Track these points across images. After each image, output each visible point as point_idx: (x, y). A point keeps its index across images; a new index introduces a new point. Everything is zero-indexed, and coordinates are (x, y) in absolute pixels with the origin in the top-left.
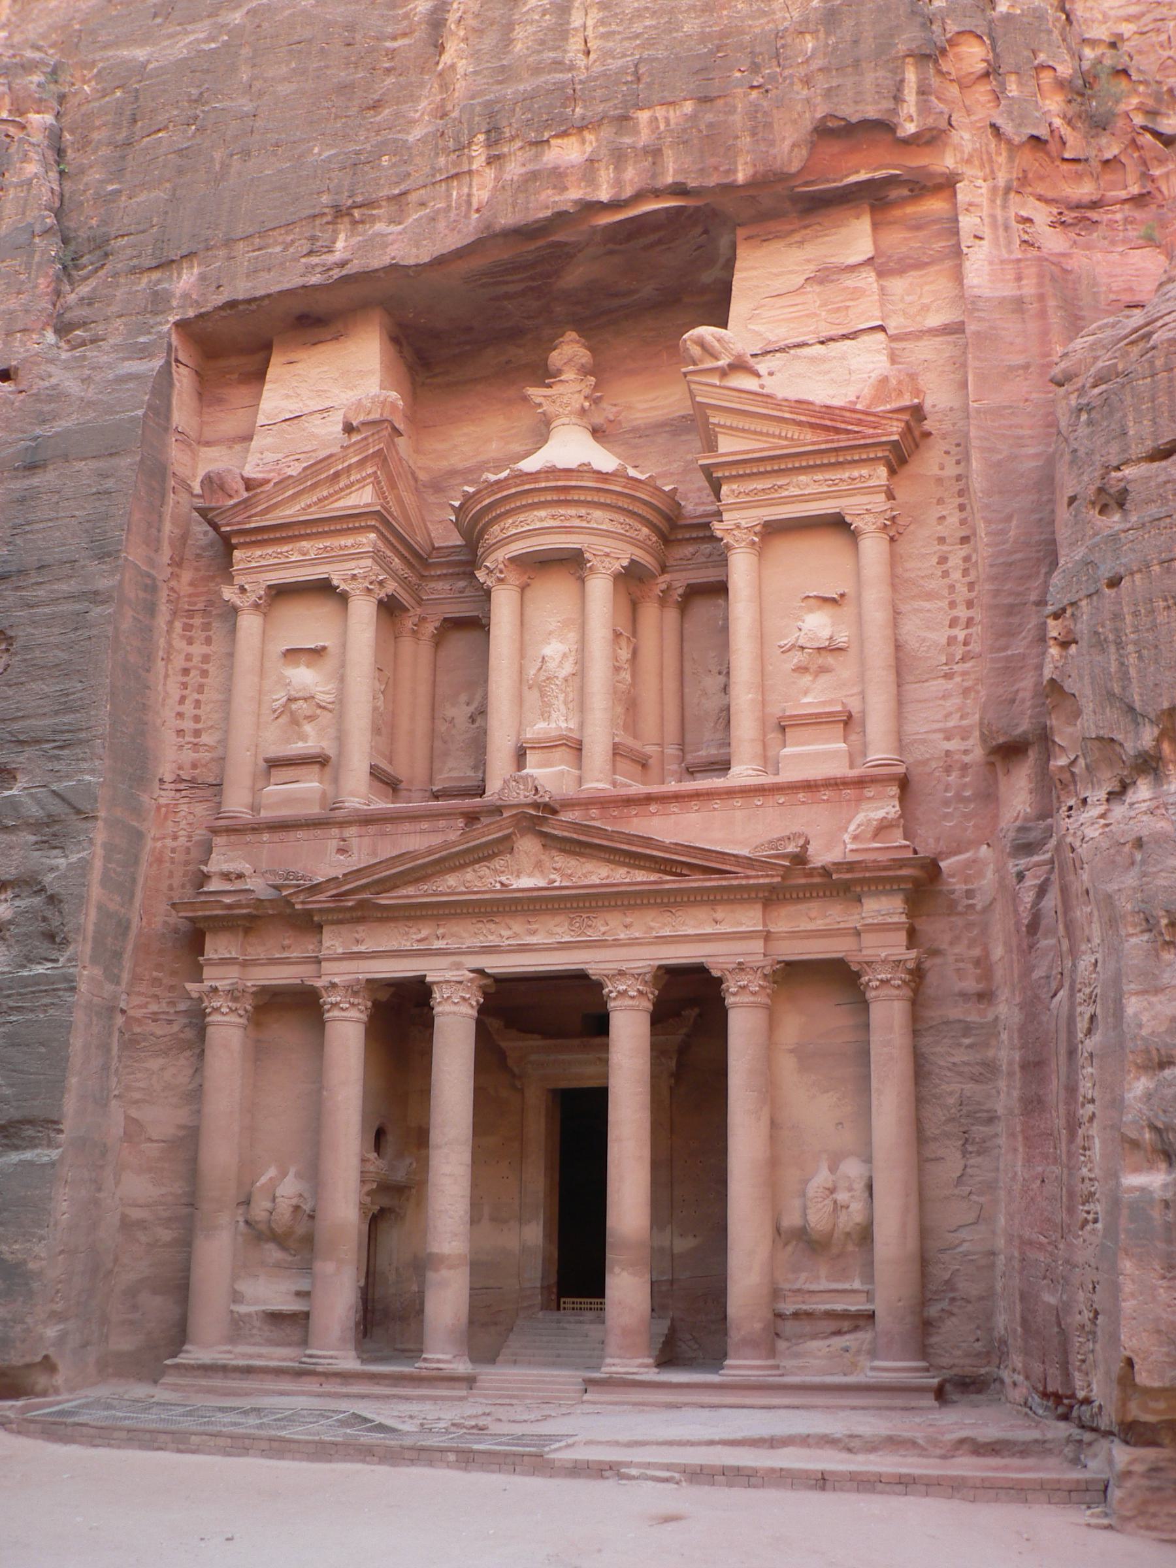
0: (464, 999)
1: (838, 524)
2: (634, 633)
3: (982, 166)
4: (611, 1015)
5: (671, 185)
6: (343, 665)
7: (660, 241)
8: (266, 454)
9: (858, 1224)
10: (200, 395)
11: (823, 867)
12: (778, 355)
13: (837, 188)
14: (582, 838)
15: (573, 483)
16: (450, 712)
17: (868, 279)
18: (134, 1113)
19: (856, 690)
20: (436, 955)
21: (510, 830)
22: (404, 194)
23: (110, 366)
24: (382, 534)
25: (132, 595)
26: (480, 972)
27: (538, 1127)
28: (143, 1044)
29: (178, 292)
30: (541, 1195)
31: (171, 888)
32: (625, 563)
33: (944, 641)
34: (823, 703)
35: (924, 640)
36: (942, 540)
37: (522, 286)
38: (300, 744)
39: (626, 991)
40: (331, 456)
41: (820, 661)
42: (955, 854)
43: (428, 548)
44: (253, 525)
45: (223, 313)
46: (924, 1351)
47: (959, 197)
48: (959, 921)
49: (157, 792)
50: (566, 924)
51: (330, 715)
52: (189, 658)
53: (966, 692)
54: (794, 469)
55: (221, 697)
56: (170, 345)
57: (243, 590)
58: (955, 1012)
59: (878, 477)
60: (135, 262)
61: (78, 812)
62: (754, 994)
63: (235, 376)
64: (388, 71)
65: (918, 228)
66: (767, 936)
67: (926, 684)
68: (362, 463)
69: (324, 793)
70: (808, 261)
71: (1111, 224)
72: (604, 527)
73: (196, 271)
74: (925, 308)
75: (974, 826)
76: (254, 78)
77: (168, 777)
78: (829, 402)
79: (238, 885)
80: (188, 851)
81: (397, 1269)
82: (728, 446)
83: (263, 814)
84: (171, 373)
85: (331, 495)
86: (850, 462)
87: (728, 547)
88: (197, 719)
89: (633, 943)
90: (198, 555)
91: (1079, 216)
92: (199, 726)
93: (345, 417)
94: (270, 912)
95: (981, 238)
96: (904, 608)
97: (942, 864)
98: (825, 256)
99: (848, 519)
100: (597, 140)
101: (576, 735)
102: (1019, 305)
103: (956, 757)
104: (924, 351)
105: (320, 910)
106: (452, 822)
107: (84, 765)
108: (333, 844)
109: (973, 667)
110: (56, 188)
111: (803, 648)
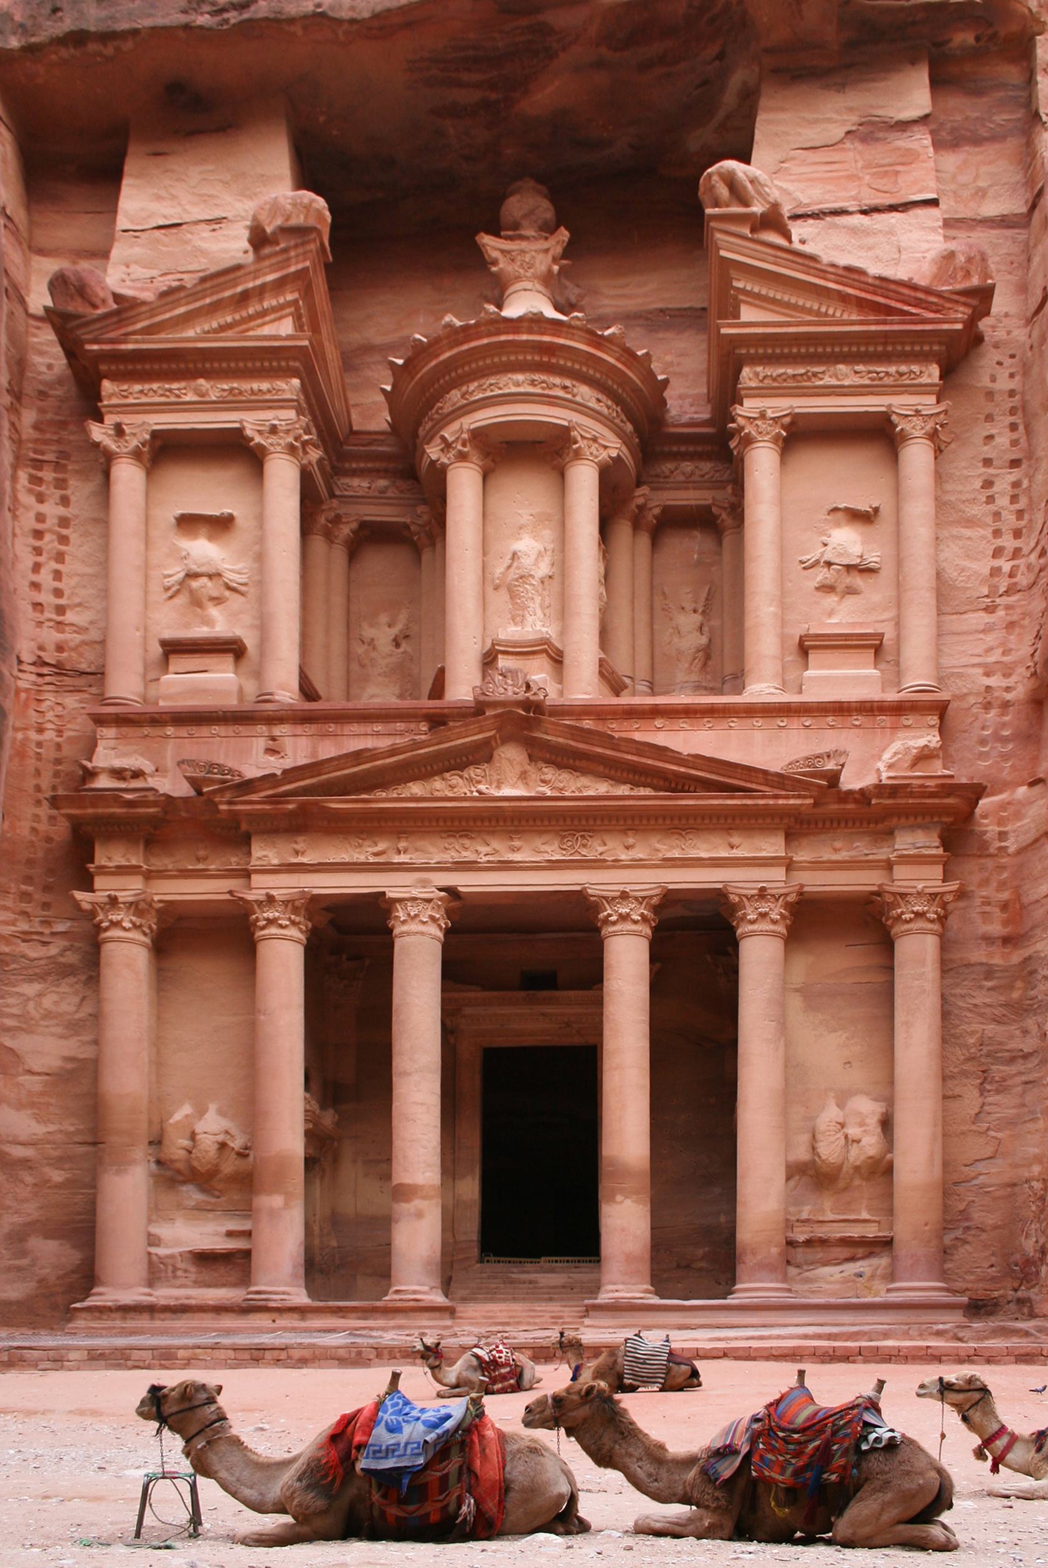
0: (432, 918)
4: (606, 942)
6: (261, 540)
12: (811, 221)
14: (581, 746)
20: (398, 870)
33: (986, 571)
35: (963, 570)
39: (628, 915)
42: (992, 794)
50: (556, 843)
53: (1011, 626)
69: (241, 690)
72: (590, 404)
75: (1011, 767)
83: (162, 703)
98: (872, 107)
103: (996, 694)
104: (982, 238)
109: (1019, 600)
111: (829, 564)
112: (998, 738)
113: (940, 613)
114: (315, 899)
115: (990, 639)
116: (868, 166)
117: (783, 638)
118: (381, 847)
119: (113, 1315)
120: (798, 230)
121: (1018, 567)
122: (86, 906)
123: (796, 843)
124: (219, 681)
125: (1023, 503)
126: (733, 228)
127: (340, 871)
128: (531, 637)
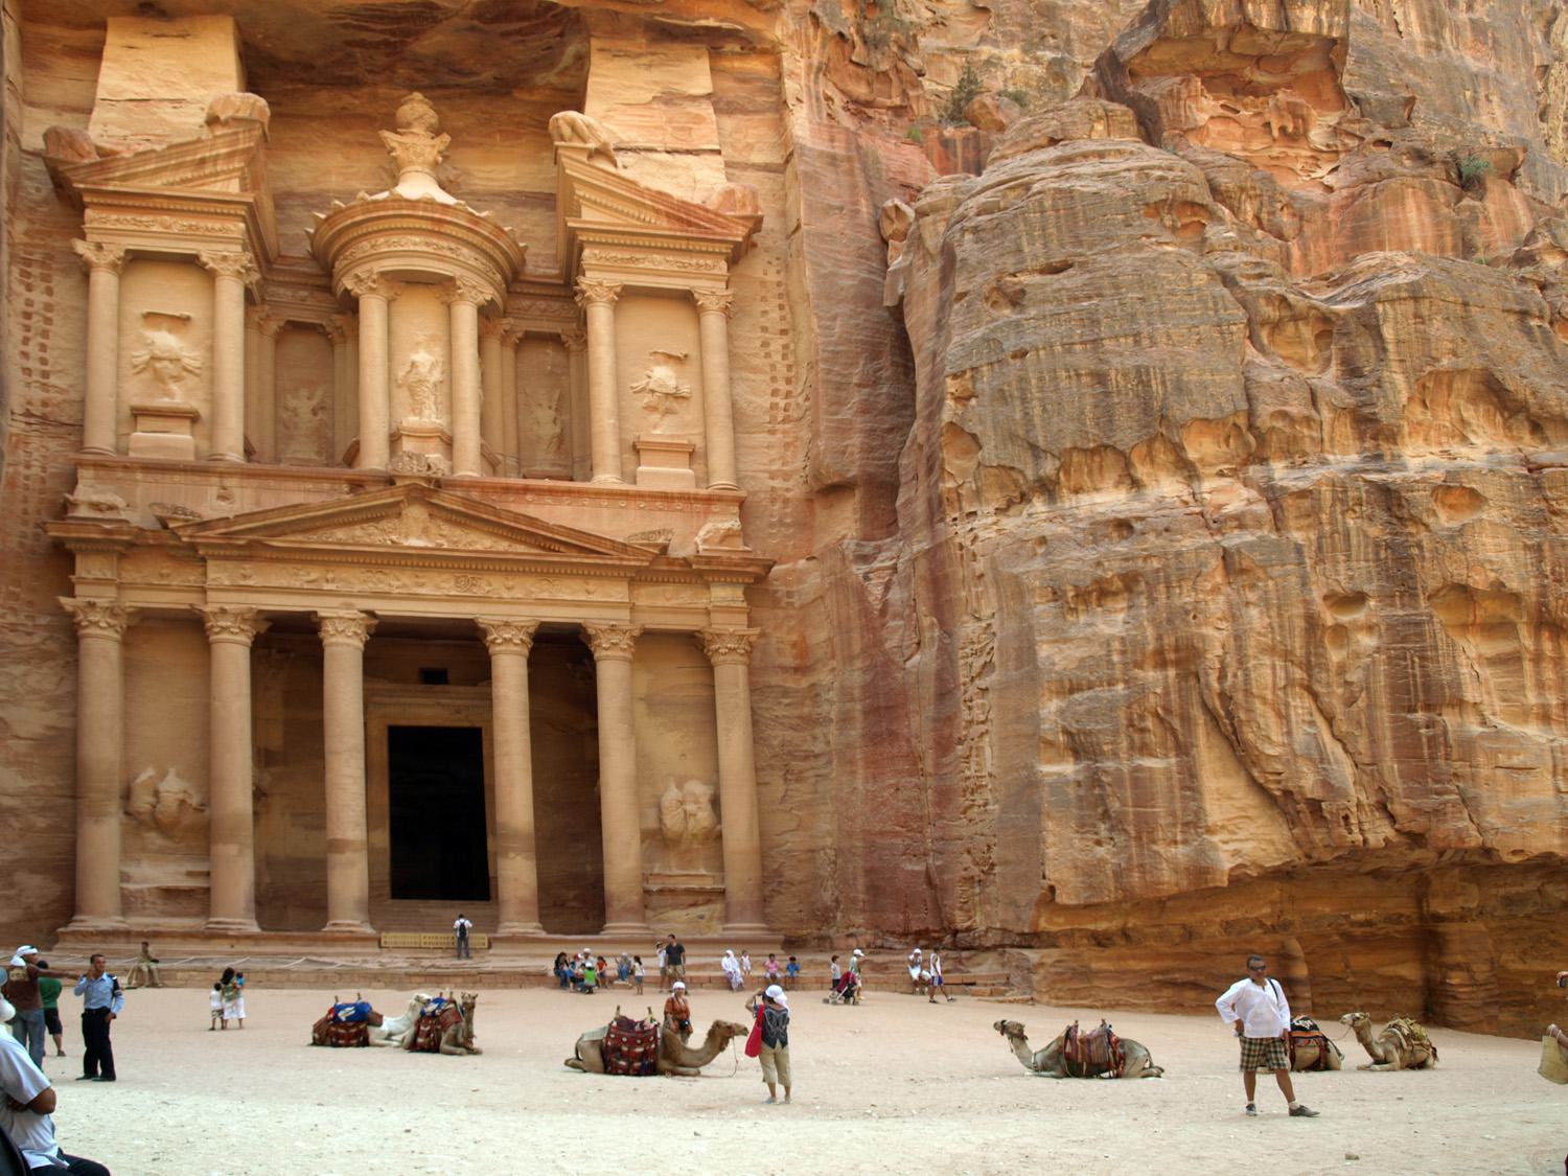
1: (686, 298)
10: (22, 56)
17: (707, 110)
19: (696, 431)
31: (26, 512)
34: (672, 436)
38: (166, 400)
39: (511, 640)
53: (787, 445)
54: (650, 247)
62: (623, 650)
63: (58, 47)
65: (744, 81)
66: (633, 608)
71: (881, 122)
80: (43, 480)
82: (590, 216)
86: (700, 252)
87: (589, 300)
88: (44, 361)
89: (515, 602)
90: (31, 209)
91: (860, 108)
92: (47, 368)
95: (799, 100)
102: (833, 160)
104: (752, 179)
111: (653, 391)
113: (735, 431)
116: (669, 121)
117: (621, 441)
118: (313, 576)
120: (620, 158)
122: (69, 609)
124: (180, 440)
126: (575, 156)
127: (283, 591)
128: (429, 426)
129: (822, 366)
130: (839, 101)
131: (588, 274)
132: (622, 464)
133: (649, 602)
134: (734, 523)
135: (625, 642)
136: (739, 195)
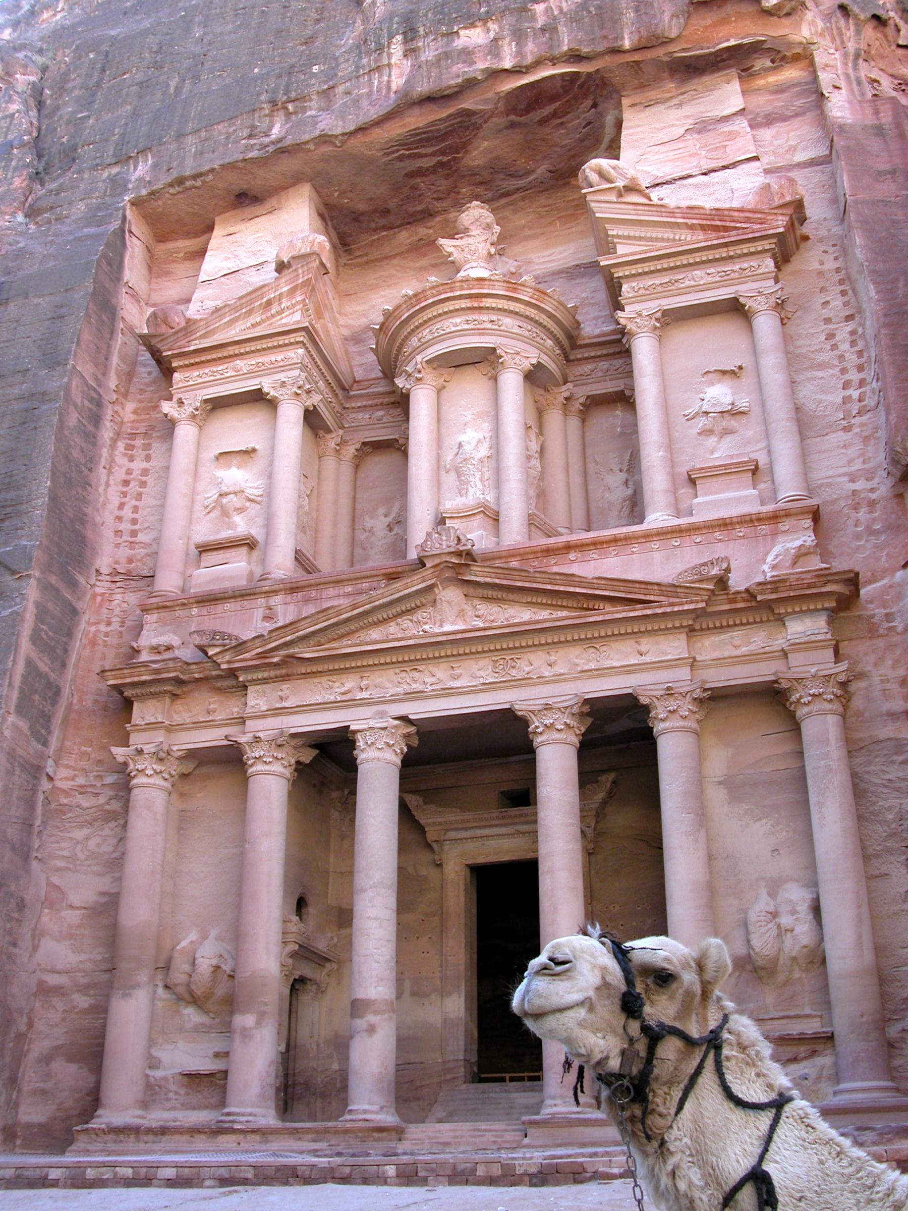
0: (389, 745)
2: (541, 432)
3: (833, 40)
5: (565, 54)
6: (271, 464)
7: (554, 115)
8: (206, 302)
9: (805, 947)
10: (150, 269)
11: (747, 590)
13: (711, 54)
14: (505, 582)
15: (485, 291)
16: (369, 523)
17: (742, 125)
18: (55, 880)
21: (433, 581)
22: (332, 88)
23: (71, 233)
24: (309, 352)
25: (79, 401)
26: (404, 719)
27: (457, 898)
28: (69, 815)
29: (133, 178)
30: (462, 967)
32: (534, 361)
33: (839, 400)
34: (732, 456)
35: (820, 402)
36: (827, 321)
37: (436, 159)
40: (264, 286)
41: (724, 424)
43: (351, 381)
44: (192, 348)
45: (172, 191)
46: (890, 1072)
47: (817, 59)
48: (880, 643)
49: (92, 581)
51: (259, 507)
52: (129, 472)
53: (866, 439)
54: (690, 265)
55: (158, 503)
56: (124, 217)
57: (181, 403)
58: (886, 731)
59: (766, 267)
60: (98, 161)
61: (13, 572)
62: (684, 718)
63: (182, 255)
64: (318, 21)
66: (693, 663)
67: (827, 437)
68: (292, 291)
70: (687, 117)
73: (150, 162)
74: (793, 149)
76: (205, 34)
77: (105, 570)
78: (718, 205)
79: (167, 655)
81: (318, 1045)
84: (124, 238)
85: (263, 321)
92: (136, 527)
93: (277, 256)
94: (197, 676)
96: (799, 378)
97: (862, 592)
99: (741, 300)
100: (500, 28)
101: (495, 507)
102: (879, 131)
103: (862, 496)
105: (246, 669)
106: (375, 584)
107: (23, 532)
108: (260, 613)
110: (35, 122)
111: (706, 413)
112: (870, 531)
114: (294, 736)
115: (852, 452)
117: (673, 476)
119: (107, 1137)
121: (865, 392)
123: (699, 645)
125: (861, 345)
129: (883, 331)
130: (887, 86)
131: (627, 308)
132: (676, 499)
133: (715, 655)
134: (807, 538)
135: (686, 706)
136: (775, 187)
